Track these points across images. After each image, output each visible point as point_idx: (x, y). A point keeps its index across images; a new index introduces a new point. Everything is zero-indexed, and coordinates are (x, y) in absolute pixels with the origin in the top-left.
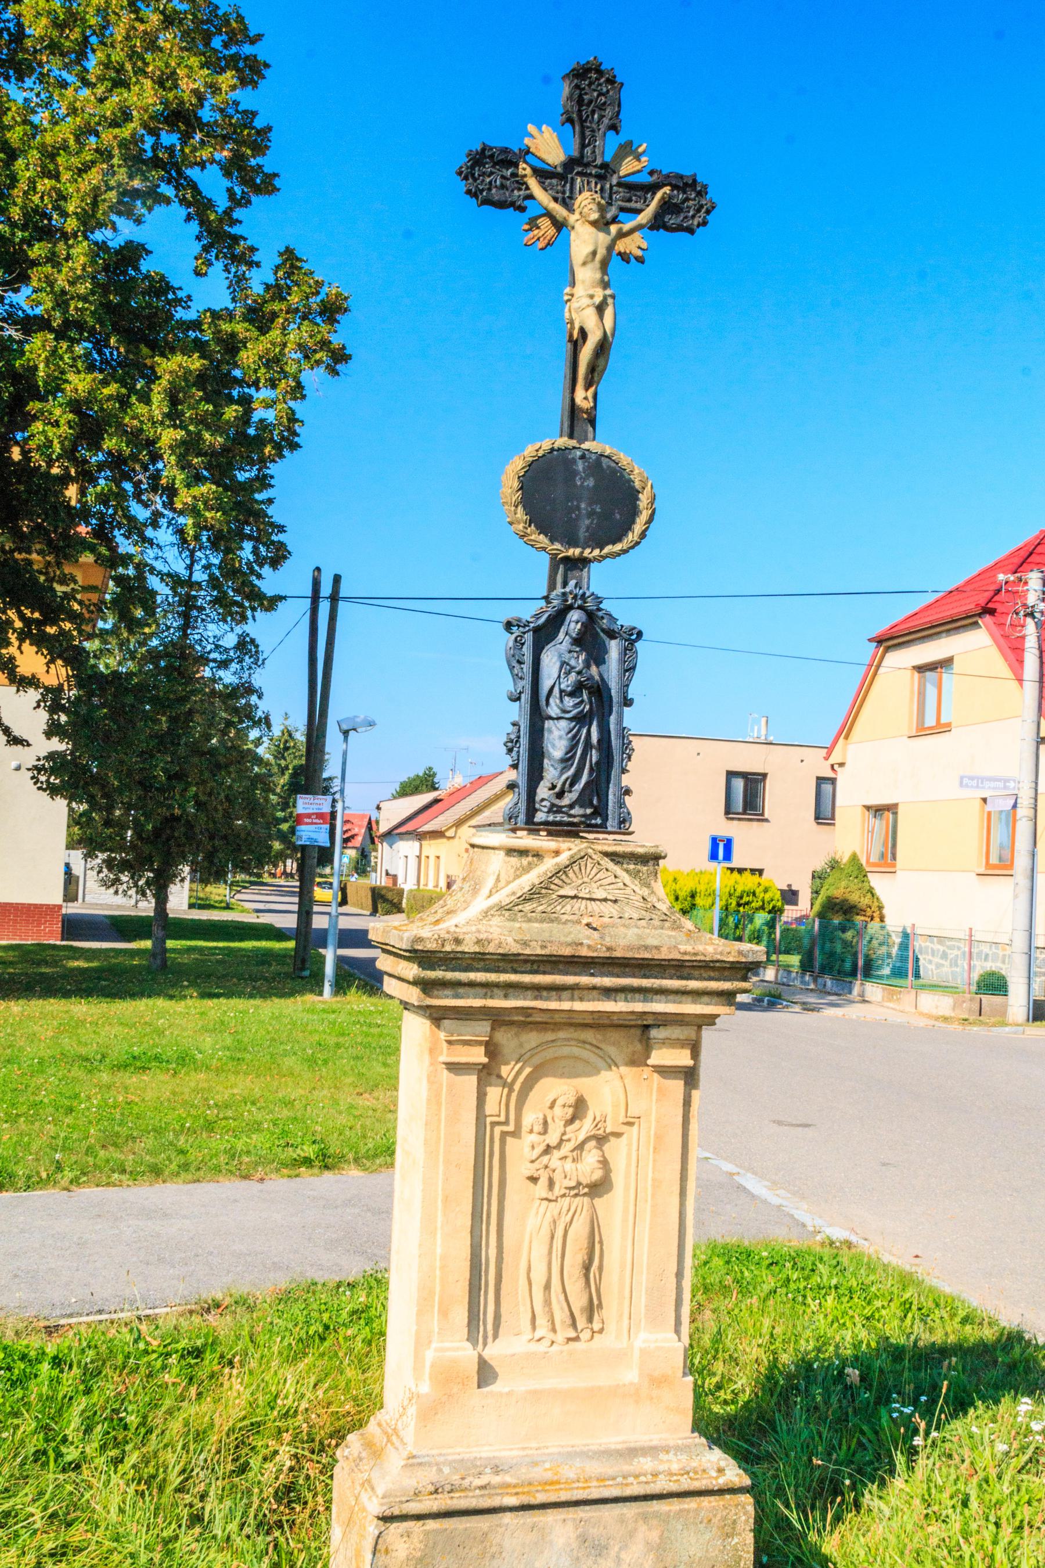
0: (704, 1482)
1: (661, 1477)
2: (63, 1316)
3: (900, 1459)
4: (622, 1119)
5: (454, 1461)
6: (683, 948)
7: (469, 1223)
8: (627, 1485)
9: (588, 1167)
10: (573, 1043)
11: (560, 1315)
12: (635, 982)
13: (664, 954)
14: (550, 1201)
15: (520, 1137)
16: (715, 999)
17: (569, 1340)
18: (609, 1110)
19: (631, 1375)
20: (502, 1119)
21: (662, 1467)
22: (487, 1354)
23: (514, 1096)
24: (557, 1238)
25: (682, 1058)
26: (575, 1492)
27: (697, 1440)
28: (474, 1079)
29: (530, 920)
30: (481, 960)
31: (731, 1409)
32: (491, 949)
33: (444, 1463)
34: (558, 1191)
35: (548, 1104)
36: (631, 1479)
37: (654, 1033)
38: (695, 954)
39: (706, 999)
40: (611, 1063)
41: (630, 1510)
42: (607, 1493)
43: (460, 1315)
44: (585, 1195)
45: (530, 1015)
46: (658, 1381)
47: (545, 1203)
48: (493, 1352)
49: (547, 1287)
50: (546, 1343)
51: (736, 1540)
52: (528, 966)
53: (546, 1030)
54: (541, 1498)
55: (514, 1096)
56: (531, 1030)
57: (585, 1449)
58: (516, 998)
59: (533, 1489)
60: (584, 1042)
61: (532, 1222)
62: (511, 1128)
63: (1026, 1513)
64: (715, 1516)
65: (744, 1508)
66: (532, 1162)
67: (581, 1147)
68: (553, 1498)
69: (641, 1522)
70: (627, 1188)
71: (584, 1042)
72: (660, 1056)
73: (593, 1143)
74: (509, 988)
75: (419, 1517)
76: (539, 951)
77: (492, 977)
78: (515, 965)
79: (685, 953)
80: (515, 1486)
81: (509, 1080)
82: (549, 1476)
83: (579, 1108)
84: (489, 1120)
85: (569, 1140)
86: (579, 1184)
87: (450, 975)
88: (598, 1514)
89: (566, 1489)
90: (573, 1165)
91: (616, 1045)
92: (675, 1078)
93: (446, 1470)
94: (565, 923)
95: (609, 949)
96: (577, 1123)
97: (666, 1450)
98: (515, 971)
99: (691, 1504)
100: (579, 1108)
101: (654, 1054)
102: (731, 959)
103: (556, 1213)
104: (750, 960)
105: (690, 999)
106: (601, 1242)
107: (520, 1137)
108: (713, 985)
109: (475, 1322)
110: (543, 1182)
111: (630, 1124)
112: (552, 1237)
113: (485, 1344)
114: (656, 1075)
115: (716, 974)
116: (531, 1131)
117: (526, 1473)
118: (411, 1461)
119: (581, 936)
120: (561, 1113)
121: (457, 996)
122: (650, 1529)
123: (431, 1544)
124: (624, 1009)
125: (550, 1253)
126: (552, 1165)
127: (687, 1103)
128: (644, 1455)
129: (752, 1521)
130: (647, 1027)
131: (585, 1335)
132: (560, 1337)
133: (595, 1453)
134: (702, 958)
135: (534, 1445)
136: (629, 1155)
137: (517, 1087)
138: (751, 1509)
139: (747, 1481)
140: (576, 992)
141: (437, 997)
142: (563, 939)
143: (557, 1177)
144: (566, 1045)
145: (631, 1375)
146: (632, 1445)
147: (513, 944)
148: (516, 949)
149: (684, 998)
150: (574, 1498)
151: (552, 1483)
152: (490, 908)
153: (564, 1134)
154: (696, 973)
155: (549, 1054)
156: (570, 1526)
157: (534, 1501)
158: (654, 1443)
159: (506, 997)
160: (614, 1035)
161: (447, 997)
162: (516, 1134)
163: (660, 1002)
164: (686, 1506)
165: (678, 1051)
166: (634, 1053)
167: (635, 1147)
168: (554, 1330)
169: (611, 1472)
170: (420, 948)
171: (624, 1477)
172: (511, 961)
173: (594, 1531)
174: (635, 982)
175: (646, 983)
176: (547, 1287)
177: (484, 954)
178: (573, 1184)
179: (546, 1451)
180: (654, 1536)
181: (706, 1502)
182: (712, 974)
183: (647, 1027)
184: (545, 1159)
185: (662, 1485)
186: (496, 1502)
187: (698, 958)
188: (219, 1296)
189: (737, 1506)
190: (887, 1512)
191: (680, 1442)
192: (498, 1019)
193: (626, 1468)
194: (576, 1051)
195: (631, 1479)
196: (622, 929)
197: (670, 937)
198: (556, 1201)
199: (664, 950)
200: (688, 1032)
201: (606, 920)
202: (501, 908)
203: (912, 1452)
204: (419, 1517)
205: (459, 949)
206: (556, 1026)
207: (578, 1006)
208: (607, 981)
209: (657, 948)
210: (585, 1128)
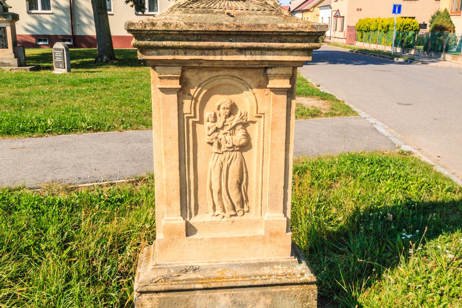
0: (293, 280)
1: (273, 276)
2: (81, 183)
3: (402, 258)
4: (255, 114)
5: (176, 267)
6: (280, 25)
7: (178, 164)
8: (255, 280)
9: (239, 137)
10: (227, 77)
11: (227, 205)
12: (255, 44)
13: (269, 29)
14: (219, 154)
15: (203, 124)
16: (301, 53)
17: (231, 216)
18: (248, 110)
19: (261, 232)
20: (192, 115)
21: (273, 273)
22: (192, 221)
23: (198, 104)
24: (224, 172)
25: (286, 84)
26: (230, 283)
27: (293, 260)
28: (176, 96)
29: (196, 13)
30: (166, 34)
31: (335, 229)
32: (172, 28)
33: (171, 268)
34: (223, 149)
35: (217, 108)
36: (258, 277)
37: (269, 71)
38: (287, 28)
39: (295, 53)
40: (249, 87)
41: (257, 291)
42: (245, 284)
43: (177, 205)
44: (237, 151)
45: (201, 63)
46: (274, 234)
47: (217, 155)
48: (194, 221)
49: (220, 192)
50: (220, 217)
51: (308, 304)
52: (195, 37)
53: (213, 71)
54: (213, 285)
55: (198, 104)
56: (205, 71)
57: (238, 263)
58: (191, 54)
59: (210, 281)
60: (234, 77)
61: (211, 164)
62: (198, 119)
63: (456, 290)
64: (298, 294)
65: (312, 290)
66: (209, 135)
67: (234, 128)
68: (219, 285)
69: (262, 296)
70: (259, 148)
71: (234, 77)
72: (274, 83)
73: (240, 126)
74: (186, 49)
75: (157, 292)
76: (198, 29)
77: (176, 43)
78: (188, 37)
79: (281, 28)
80: (202, 280)
81: (195, 96)
82: (219, 275)
83: (233, 109)
84: (185, 116)
85: (228, 125)
86: (234, 146)
87: (152, 43)
88: (241, 292)
89: (226, 281)
90: (230, 137)
91: (251, 78)
92: (282, 94)
93: (172, 271)
94: (216, 14)
95: (238, 26)
96: (232, 117)
97: (278, 264)
98: (188, 40)
99: (287, 289)
100: (233, 109)
101: (270, 82)
102: (307, 30)
103: (222, 159)
104: (319, 30)
105: (286, 53)
106: (247, 172)
107: (203, 124)
108: (299, 45)
109: (185, 208)
110: (215, 144)
111: (260, 117)
112: (221, 170)
113: (191, 217)
114: (272, 92)
115: (300, 39)
116: (208, 121)
117: (209, 274)
118: (156, 267)
119: (223, 20)
120: (223, 112)
121: (159, 54)
122: (266, 299)
123: (162, 303)
124: (250, 59)
125: (220, 177)
126: (220, 137)
127: (289, 106)
128: (266, 266)
129: (316, 296)
130: (266, 68)
131: (240, 213)
132: (227, 215)
133: (243, 264)
134: (291, 30)
135: (215, 261)
136: (259, 131)
137: (199, 99)
138: (316, 291)
139: (314, 279)
140: (224, 51)
141: (149, 55)
142: (212, 22)
143: (223, 142)
144: (224, 78)
145: (261, 232)
146: (261, 261)
147: (184, 25)
148: (186, 28)
149: (283, 52)
150: (229, 286)
151: (220, 279)
152: (174, 6)
153: (225, 122)
154: (289, 39)
155: (216, 83)
156: (228, 297)
157: (209, 286)
158: (272, 260)
159: (185, 54)
160: (250, 73)
161: (154, 55)
162: (201, 122)
163: (270, 55)
164: (284, 290)
165: (283, 80)
166: (260, 81)
167: (262, 128)
168: (224, 211)
169: (248, 274)
170: (133, 28)
171: (255, 276)
172: (185, 35)
173: (239, 299)
174: (255, 44)
175: (260, 45)
176: (220, 192)
177: (168, 31)
178: (231, 145)
179: (220, 263)
180: (269, 301)
181: (294, 288)
182: (298, 39)
183: (266, 68)
184: (216, 134)
185: (273, 280)
186: (192, 286)
187: (289, 30)
188: (144, 175)
189: (309, 290)
190: (392, 281)
191: (285, 260)
192: (185, 66)
193: (256, 272)
194: (229, 81)
195: (258, 277)
196: (248, 16)
197: (274, 19)
198: (222, 153)
199: (269, 26)
200: (289, 71)
201: (239, 11)
202: (180, 6)
203: (407, 256)
204: (157, 292)
205: (154, 29)
206: (218, 69)
207: (225, 58)
208: (239, 44)
209: (265, 25)
210: (236, 119)
